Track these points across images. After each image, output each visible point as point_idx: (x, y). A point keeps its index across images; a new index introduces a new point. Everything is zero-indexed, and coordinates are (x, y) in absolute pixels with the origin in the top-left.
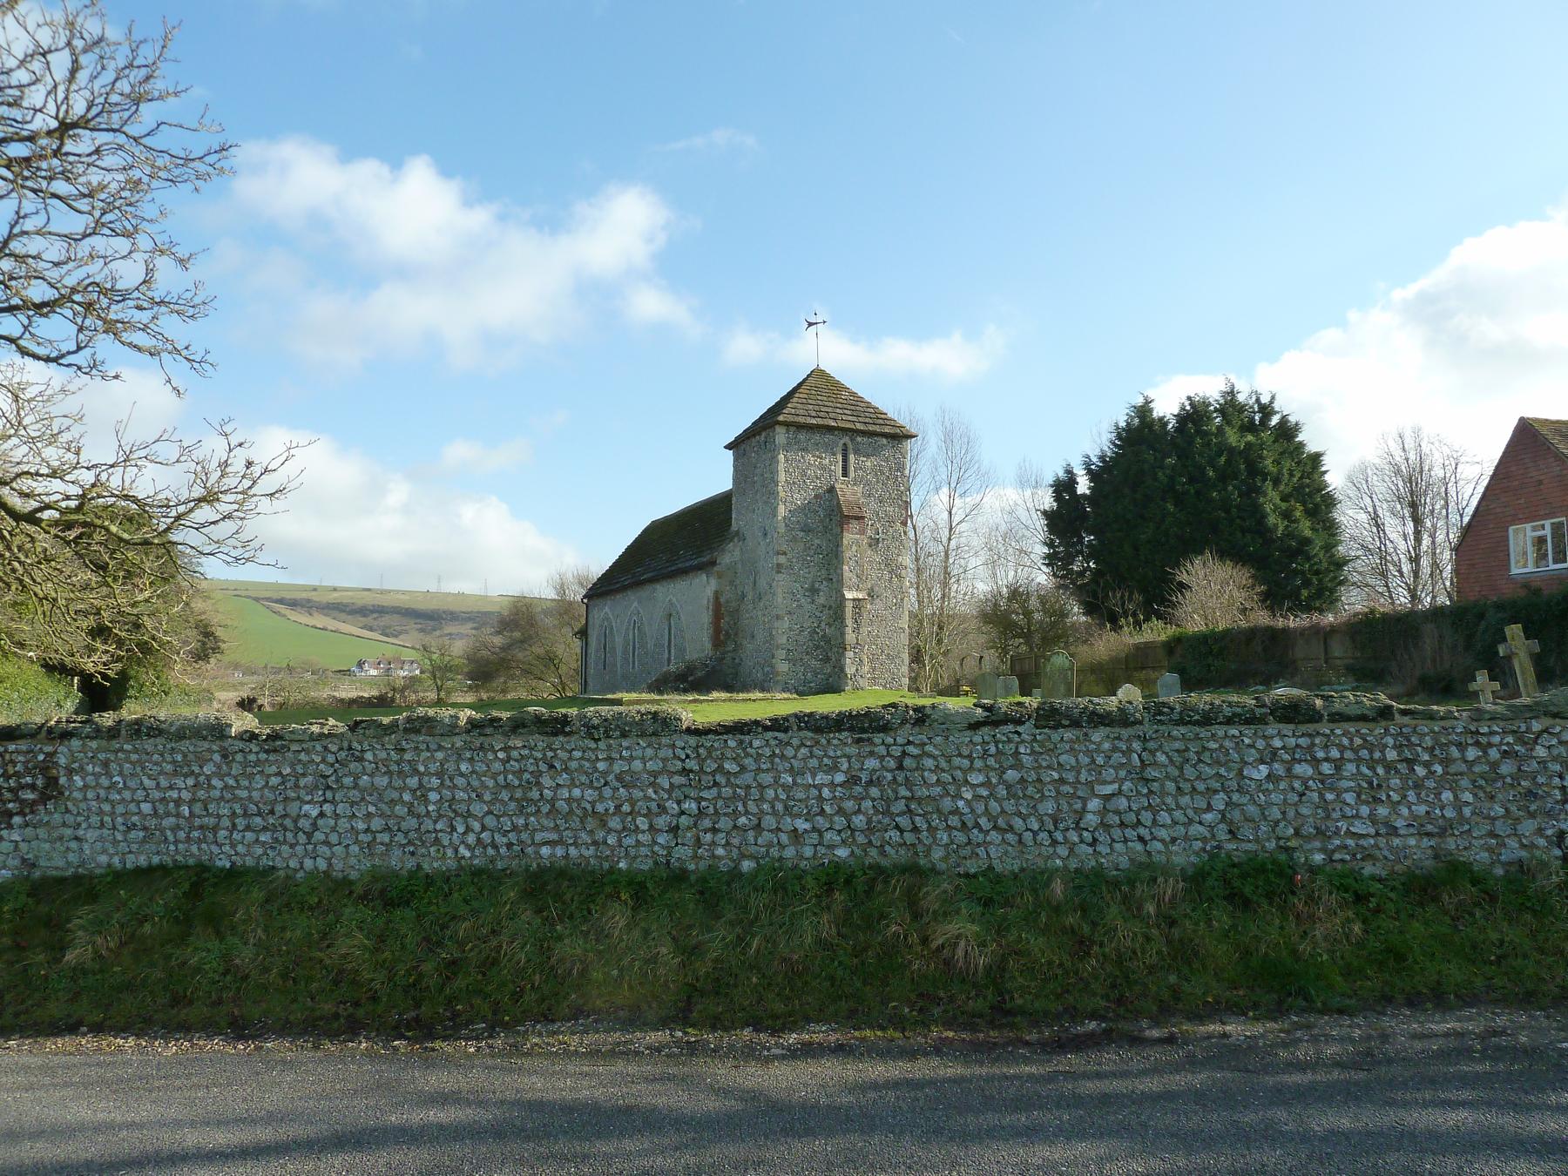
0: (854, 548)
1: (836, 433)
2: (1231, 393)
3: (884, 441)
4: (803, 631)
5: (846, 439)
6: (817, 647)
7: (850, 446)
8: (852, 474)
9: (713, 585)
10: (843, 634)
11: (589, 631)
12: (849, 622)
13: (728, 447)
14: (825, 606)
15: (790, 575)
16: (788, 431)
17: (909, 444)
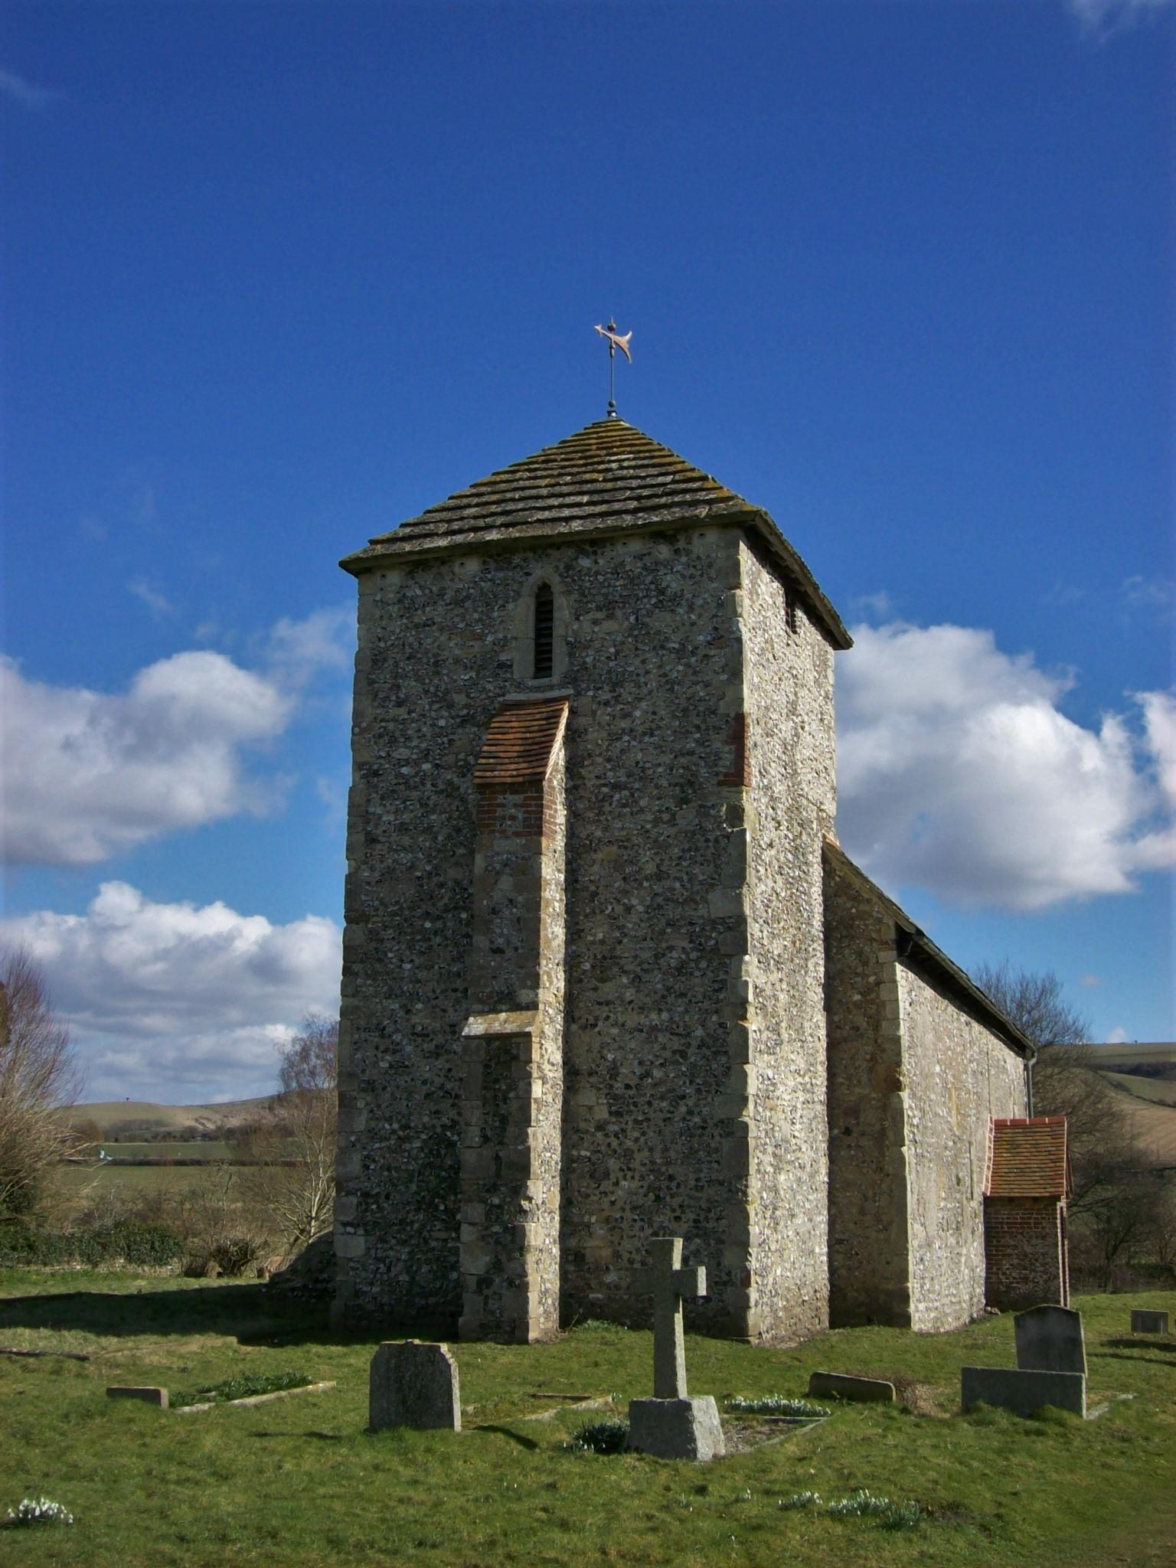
1: (517, 560)
8: (560, 662)
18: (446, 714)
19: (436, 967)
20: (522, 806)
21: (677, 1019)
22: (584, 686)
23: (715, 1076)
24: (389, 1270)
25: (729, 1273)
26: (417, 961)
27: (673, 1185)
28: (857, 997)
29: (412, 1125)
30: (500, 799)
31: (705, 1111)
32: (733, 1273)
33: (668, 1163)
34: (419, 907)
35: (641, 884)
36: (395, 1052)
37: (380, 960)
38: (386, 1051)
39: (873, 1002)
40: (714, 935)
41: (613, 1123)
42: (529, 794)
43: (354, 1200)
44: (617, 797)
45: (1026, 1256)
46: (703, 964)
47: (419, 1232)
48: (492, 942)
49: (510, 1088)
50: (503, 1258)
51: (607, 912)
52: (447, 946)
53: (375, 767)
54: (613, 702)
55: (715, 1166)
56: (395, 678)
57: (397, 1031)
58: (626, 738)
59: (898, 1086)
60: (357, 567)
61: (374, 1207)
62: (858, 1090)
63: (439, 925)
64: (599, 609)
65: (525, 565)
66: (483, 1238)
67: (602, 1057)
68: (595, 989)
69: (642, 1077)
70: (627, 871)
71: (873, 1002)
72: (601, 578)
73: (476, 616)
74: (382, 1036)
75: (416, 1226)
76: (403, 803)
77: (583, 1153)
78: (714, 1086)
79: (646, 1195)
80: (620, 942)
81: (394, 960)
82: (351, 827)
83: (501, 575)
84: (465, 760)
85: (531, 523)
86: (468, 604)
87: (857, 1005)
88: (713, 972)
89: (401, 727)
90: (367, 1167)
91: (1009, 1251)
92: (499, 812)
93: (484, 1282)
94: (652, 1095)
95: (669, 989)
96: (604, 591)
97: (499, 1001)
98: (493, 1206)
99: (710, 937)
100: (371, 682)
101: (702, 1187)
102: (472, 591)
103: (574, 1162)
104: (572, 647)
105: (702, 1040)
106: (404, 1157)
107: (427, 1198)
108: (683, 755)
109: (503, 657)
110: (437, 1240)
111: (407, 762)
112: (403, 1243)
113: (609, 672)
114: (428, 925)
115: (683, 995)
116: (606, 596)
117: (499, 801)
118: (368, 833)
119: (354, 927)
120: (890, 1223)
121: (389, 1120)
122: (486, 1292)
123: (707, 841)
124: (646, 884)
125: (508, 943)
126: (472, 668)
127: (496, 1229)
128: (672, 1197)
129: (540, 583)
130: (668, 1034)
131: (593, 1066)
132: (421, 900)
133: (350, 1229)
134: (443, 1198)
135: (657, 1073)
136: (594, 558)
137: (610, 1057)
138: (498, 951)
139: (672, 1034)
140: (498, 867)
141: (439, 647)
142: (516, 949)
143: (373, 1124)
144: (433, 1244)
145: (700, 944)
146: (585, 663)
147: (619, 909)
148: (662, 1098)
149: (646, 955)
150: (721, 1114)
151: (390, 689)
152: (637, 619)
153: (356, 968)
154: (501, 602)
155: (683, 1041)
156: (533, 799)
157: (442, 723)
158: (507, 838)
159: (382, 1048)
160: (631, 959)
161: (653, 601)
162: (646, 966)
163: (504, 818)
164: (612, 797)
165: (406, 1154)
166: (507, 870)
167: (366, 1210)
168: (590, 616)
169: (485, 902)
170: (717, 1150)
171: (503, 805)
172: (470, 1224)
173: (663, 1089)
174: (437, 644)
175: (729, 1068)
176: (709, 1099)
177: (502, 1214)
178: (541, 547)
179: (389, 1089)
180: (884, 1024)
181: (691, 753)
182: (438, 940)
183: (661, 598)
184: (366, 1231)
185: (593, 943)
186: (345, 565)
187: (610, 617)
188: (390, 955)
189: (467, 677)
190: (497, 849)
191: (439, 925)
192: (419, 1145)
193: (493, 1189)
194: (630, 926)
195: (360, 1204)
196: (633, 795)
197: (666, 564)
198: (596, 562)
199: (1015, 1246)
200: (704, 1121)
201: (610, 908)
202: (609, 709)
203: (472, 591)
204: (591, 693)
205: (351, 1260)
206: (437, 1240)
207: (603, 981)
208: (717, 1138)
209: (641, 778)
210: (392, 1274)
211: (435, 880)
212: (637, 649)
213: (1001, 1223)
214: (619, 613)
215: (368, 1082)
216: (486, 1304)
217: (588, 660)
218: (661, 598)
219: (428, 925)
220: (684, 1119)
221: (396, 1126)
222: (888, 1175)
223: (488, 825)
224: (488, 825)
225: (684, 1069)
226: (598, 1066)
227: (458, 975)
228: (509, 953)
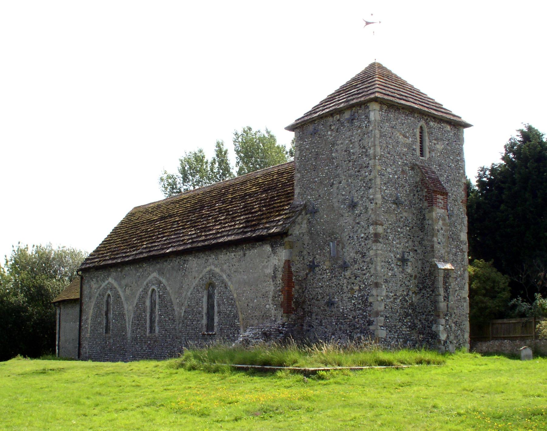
0: (441, 222)
2: (522, 132)
3: (448, 128)
6: (407, 315)
7: (426, 130)
8: (427, 155)
9: (283, 254)
10: (435, 303)
11: (85, 300)
12: (442, 291)
13: (291, 128)
14: (411, 276)
16: (381, 109)
17: (466, 130)
20: (443, 200)
36: (392, 270)
52: (404, 237)
74: (389, 265)
92: (438, 200)
98: (447, 320)
115: (456, 261)
118: (382, 196)
121: (391, 292)
133: (382, 328)
138: (439, 243)
144: (404, 332)
151: (385, 147)
156: (445, 198)
159: (389, 268)
172: (442, 325)
182: (402, 235)
193: (446, 315)
215: (386, 280)
216: (446, 348)
219: (399, 230)
227: (407, 247)
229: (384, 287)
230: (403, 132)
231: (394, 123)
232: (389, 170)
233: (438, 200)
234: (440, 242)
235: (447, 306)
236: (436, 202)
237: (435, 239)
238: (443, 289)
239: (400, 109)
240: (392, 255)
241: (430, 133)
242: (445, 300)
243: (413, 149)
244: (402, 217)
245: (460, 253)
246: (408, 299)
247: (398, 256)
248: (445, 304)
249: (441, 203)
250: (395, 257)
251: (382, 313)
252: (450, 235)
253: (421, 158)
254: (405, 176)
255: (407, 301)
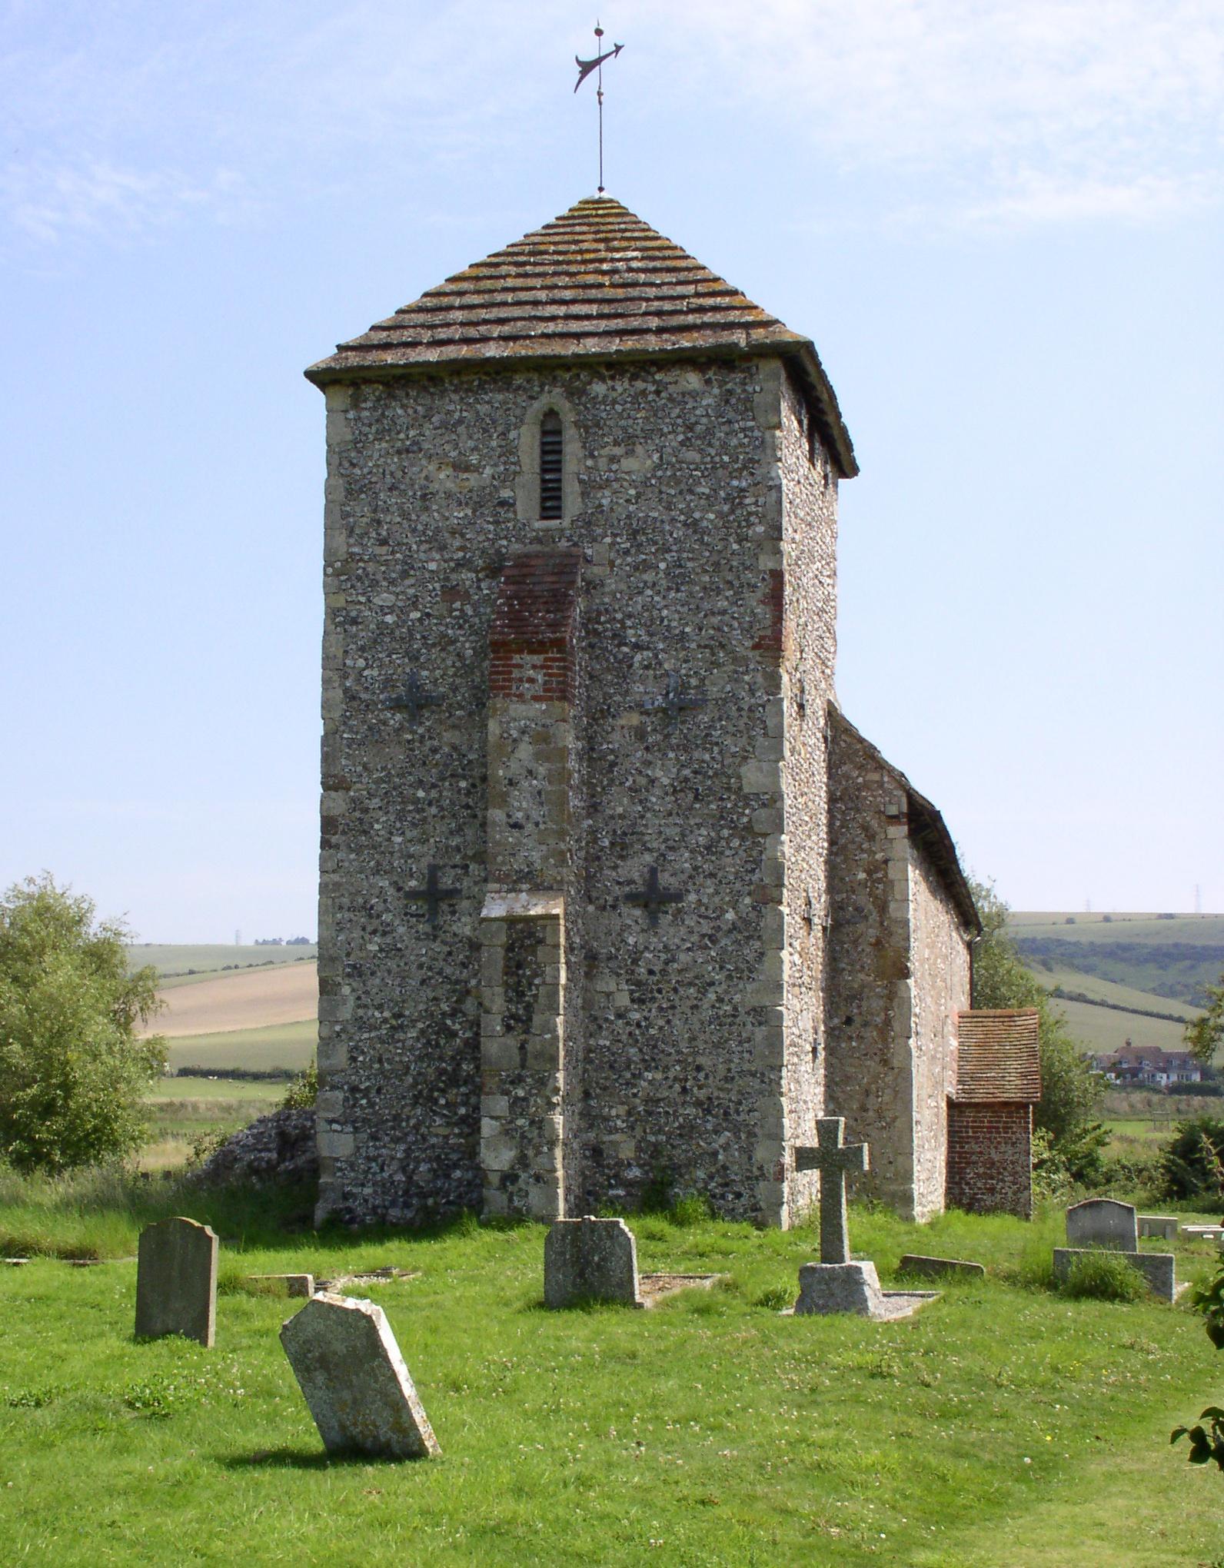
0: (525, 751)
1: (519, 380)
3: (692, 380)
4: (401, 1027)
5: (554, 397)
7: (568, 416)
8: (572, 503)
15: (358, 851)
18: (438, 557)
19: (432, 840)
20: (543, 667)
21: (705, 900)
22: (599, 531)
23: (748, 962)
24: (382, 1170)
25: (761, 1168)
26: (409, 835)
27: (701, 1076)
28: (862, 876)
29: (407, 1013)
30: (516, 659)
31: (737, 998)
32: (766, 1166)
33: (696, 1053)
34: (410, 774)
35: (665, 754)
36: (384, 934)
37: (365, 832)
38: (374, 932)
39: (879, 881)
40: (747, 812)
41: (635, 1010)
42: (550, 655)
43: (340, 1095)
44: (638, 657)
45: (993, 1164)
46: (736, 843)
47: (416, 1127)
48: (509, 816)
49: (535, 975)
50: (530, 1153)
51: (627, 784)
52: (443, 817)
53: (354, 614)
54: (633, 551)
55: (746, 1055)
56: (375, 511)
57: (388, 910)
58: (649, 592)
59: (906, 973)
60: (320, 377)
61: (364, 1102)
62: (861, 976)
63: (434, 794)
64: (616, 443)
65: (528, 386)
66: (507, 1132)
67: (623, 941)
68: (615, 867)
69: (667, 963)
70: (650, 740)
71: (879, 881)
72: (619, 408)
73: (471, 444)
74: (370, 916)
75: (412, 1122)
76: (389, 656)
77: (601, 1042)
78: (746, 973)
79: (671, 1087)
80: (642, 817)
81: (382, 833)
82: (326, 682)
83: (500, 397)
84: (462, 610)
85: (529, 337)
86: (461, 429)
87: (863, 884)
88: (745, 851)
89: (383, 568)
90: (354, 1059)
91: (974, 1158)
92: (516, 673)
93: (509, 1178)
94: (678, 982)
95: (695, 868)
96: (623, 423)
97: (519, 881)
98: (517, 1099)
99: (743, 814)
100: (345, 515)
101: (733, 1078)
102: (465, 414)
103: (591, 1051)
104: (588, 488)
105: (733, 924)
106: (398, 1048)
107: (425, 1092)
108: (713, 614)
109: (506, 494)
110: (437, 1136)
111: (391, 610)
112: (397, 1140)
113: (628, 517)
114: (421, 794)
115: (712, 875)
116: (624, 429)
117: (514, 662)
118: (346, 690)
119: (333, 794)
120: (895, 1119)
121: (380, 1007)
122: (510, 1188)
123: (740, 709)
124: (671, 755)
125: (528, 818)
126: (467, 504)
127: (520, 1122)
128: (700, 1088)
129: (546, 409)
130: (695, 917)
131: (613, 950)
132: (413, 766)
133: (335, 1126)
134: (443, 1091)
135: (684, 957)
136: (610, 383)
137: (631, 940)
138: (516, 826)
139: (700, 916)
140: (515, 734)
141: (427, 478)
142: (537, 824)
143: (361, 1012)
144: (433, 1140)
145: (732, 821)
146: (601, 505)
147: (642, 781)
148: (691, 984)
149: (673, 832)
150: (752, 1001)
152: (661, 458)
153: (334, 839)
154: (500, 429)
155: (712, 925)
157: (433, 566)
158: (524, 702)
159: (369, 929)
160: (654, 836)
161: (681, 437)
162: (671, 843)
163: (521, 680)
164: (632, 657)
165: (400, 1045)
166: (526, 738)
167: (354, 1106)
168: (605, 451)
169: (501, 772)
170: (749, 1040)
171: (520, 666)
172: (492, 1118)
173: (690, 975)
174: (423, 475)
175: (762, 954)
176: (741, 986)
177: (528, 1107)
178: (546, 368)
179: (379, 974)
180: (892, 906)
181: (724, 612)
182: (434, 810)
183: (689, 435)
184: (356, 1128)
185: (612, 817)
186: (312, 375)
187: (630, 453)
188: (376, 826)
189: (461, 515)
190: (512, 714)
191: (434, 794)
192: (415, 1035)
193: (518, 1081)
194: (654, 800)
195: (346, 1099)
196: (656, 656)
197: (694, 395)
198: (613, 389)
199: (981, 1153)
200: (735, 1009)
201: (631, 779)
202: (629, 559)
203: (465, 414)
204: (608, 540)
205: (337, 1160)
206: (437, 1136)
207: (622, 857)
208: (749, 1027)
209: (666, 638)
210: (386, 1175)
211: (428, 743)
212: (661, 492)
213: (967, 1127)
214: (639, 449)
215: (354, 967)
216: (511, 1200)
217: (605, 502)
218: (689, 435)
219: (421, 794)
220: (713, 1007)
221: (387, 1014)
222: (893, 1069)
223: (503, 688)
224: (503, 688)
225: (713, 954)
226: (618, 950)
227: (458, 849)
228: (529, 827)
229: (346, 990)
230: (453, 454)
231: (412, 433)
232: (384, 598)
233: (516, 673)
234: (523, 821)
235: (522, 1048)
236: (509, 680)
237: (497, 815)
238: (500, 990)
239: (442, 380)
240: (384, 883)
241: (589, 428)
242: (509, 1028)
243: (503, 503)
244: (434, 751)
245: (736, 843)
246: (457, 1027)
247: (413, 883)
248: (512, 1042)
249: (531, 680)
250: (399, 889)
251: (336, 1078)
252: (686, 780)
253: (539, 524)
254: (457, 605)
255: (454, 1034)
